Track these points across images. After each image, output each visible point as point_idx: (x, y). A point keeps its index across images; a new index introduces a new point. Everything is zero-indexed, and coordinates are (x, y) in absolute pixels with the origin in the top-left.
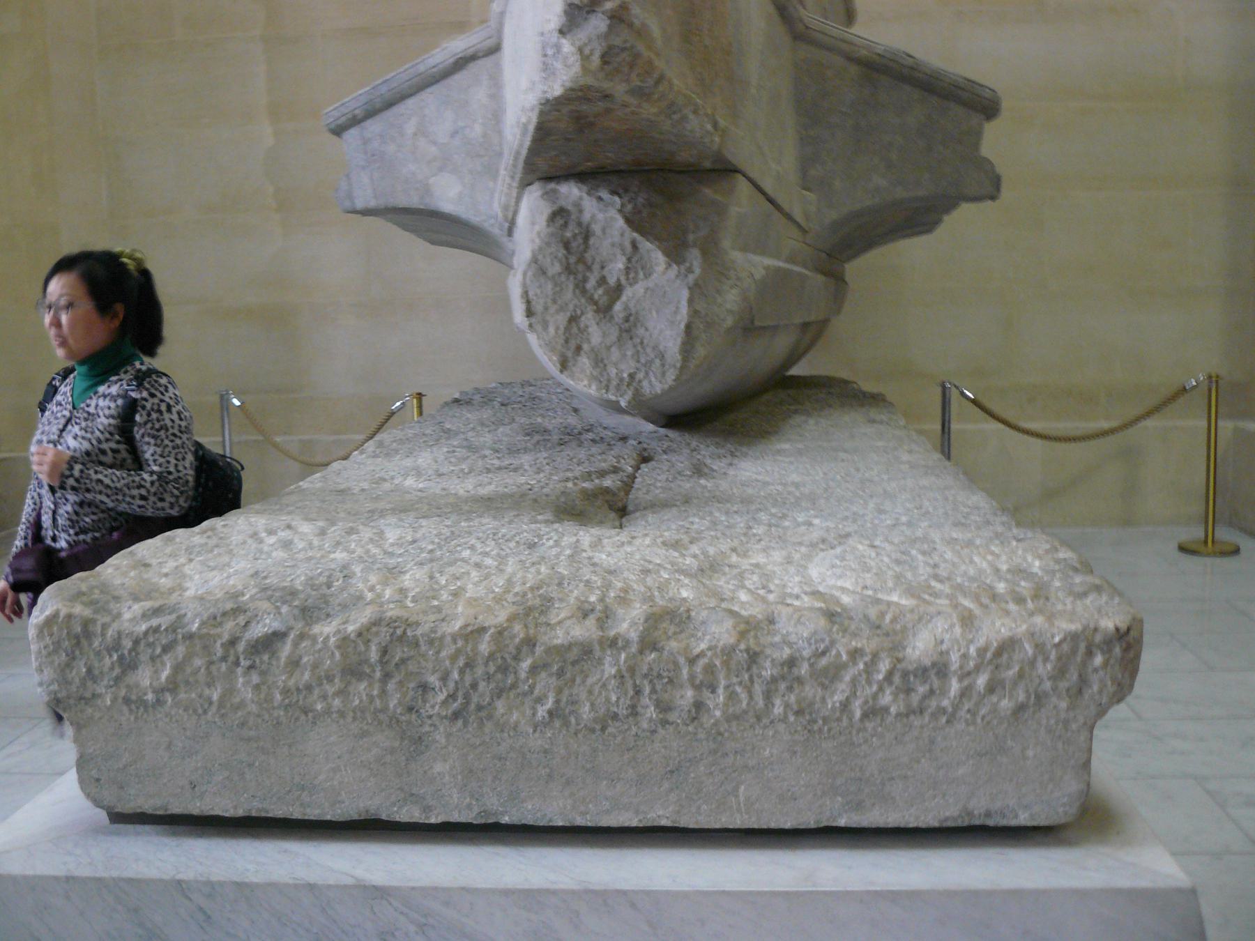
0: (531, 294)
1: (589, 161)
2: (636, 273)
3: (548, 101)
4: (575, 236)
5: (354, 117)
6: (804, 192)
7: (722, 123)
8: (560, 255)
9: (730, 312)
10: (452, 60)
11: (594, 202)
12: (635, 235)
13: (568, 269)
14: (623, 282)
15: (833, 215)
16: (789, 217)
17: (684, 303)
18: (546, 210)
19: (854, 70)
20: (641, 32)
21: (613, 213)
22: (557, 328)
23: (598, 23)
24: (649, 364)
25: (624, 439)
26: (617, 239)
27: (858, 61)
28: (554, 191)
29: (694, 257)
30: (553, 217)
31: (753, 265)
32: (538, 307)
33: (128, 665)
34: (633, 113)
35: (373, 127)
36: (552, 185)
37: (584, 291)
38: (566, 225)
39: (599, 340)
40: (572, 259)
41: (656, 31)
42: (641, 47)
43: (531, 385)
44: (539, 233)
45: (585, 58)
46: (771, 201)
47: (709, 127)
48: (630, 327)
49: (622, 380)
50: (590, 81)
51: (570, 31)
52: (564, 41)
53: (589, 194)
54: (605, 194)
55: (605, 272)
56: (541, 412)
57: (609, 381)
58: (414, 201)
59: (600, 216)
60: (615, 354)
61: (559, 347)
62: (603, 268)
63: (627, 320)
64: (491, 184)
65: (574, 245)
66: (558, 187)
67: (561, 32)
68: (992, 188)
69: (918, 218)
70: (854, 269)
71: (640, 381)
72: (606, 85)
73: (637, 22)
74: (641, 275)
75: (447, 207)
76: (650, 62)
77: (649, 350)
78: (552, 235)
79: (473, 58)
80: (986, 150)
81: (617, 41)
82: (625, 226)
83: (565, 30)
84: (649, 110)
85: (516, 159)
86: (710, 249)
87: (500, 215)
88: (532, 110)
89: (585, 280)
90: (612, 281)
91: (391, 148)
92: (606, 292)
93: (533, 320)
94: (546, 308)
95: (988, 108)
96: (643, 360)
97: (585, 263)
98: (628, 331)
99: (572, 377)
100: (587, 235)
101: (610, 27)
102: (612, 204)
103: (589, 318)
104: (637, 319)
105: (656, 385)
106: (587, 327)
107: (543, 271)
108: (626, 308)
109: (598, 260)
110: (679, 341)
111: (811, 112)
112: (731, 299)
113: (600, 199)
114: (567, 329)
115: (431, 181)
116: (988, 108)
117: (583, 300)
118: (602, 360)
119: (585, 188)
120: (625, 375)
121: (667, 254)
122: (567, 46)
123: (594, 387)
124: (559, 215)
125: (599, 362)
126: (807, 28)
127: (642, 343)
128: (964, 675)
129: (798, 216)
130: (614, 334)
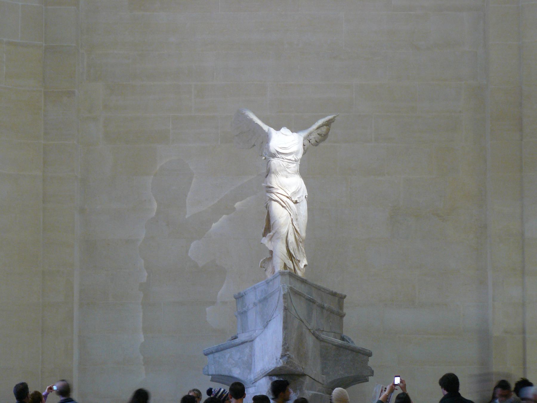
15: (330, 380)
19: (334, 347)
23: (286, 358)
27: (335, 345)
29: (298, 391)
35: (217, 355)
41: (293, 356)
58: (226, 373)
64: (248, 371)
79: (246, 342)
84: (292, 368)
87: (253, 379)
95: (370, 355)
111: (324, 357)
116: (370, 355)
129: (321, 381)
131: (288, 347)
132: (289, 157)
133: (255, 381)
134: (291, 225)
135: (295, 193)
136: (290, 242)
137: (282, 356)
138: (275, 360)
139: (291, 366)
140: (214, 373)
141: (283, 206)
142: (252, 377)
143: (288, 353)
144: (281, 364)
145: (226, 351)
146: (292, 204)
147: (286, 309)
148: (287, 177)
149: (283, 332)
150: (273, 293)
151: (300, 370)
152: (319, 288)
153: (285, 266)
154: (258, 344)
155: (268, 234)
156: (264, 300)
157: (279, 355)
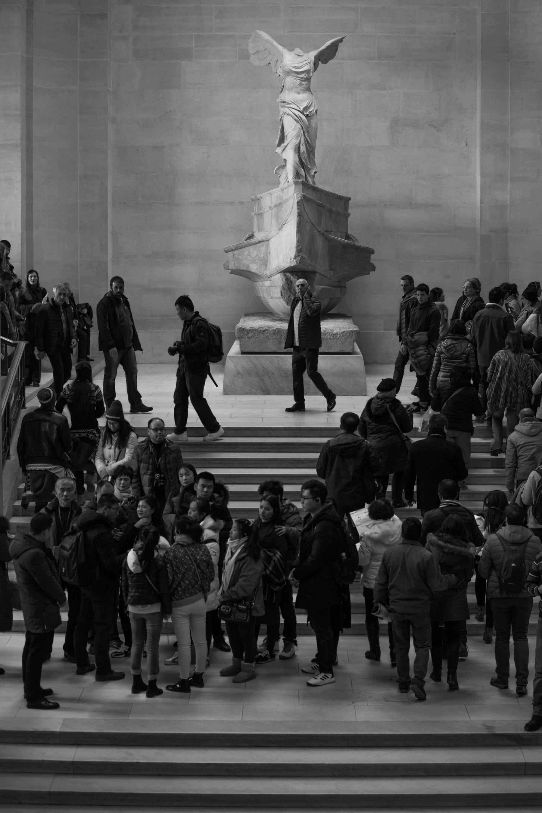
13: (288, 288)
30: (286, 280)
33: (248, 333)
35: (236, 252)
58: (245, 269)
68: (374, 269)
70: (349, 284)
75: (253, 271)
84: (304, 267)
87: (268, 274)
91: (240, 257)
95: (372, 252)
100: (292, 282)
116: (372, 252)
124: (287, 279)
128: (340, 335)
129: (328, 276)
131: (301, 249)
132: (302, 76)
133: (271, 276)
134: (303, 137)
135: (306, 108)
136: (301, 151)
137: (295, 257)
139: (303, 265)
140: (234, 268)
141: (295, 120)
142: (268, 273)
144: (294, 263)
145: (244, 249)
146: (304, 117)
147: (300, 215)
148: (299, 94)
150: (287, 200)
151: (310, 268)
152: (327, 194)
153: (297, 175)
154: (273, 244)
155: (283, 145)
156: (279, 205)
157: (293, 257)
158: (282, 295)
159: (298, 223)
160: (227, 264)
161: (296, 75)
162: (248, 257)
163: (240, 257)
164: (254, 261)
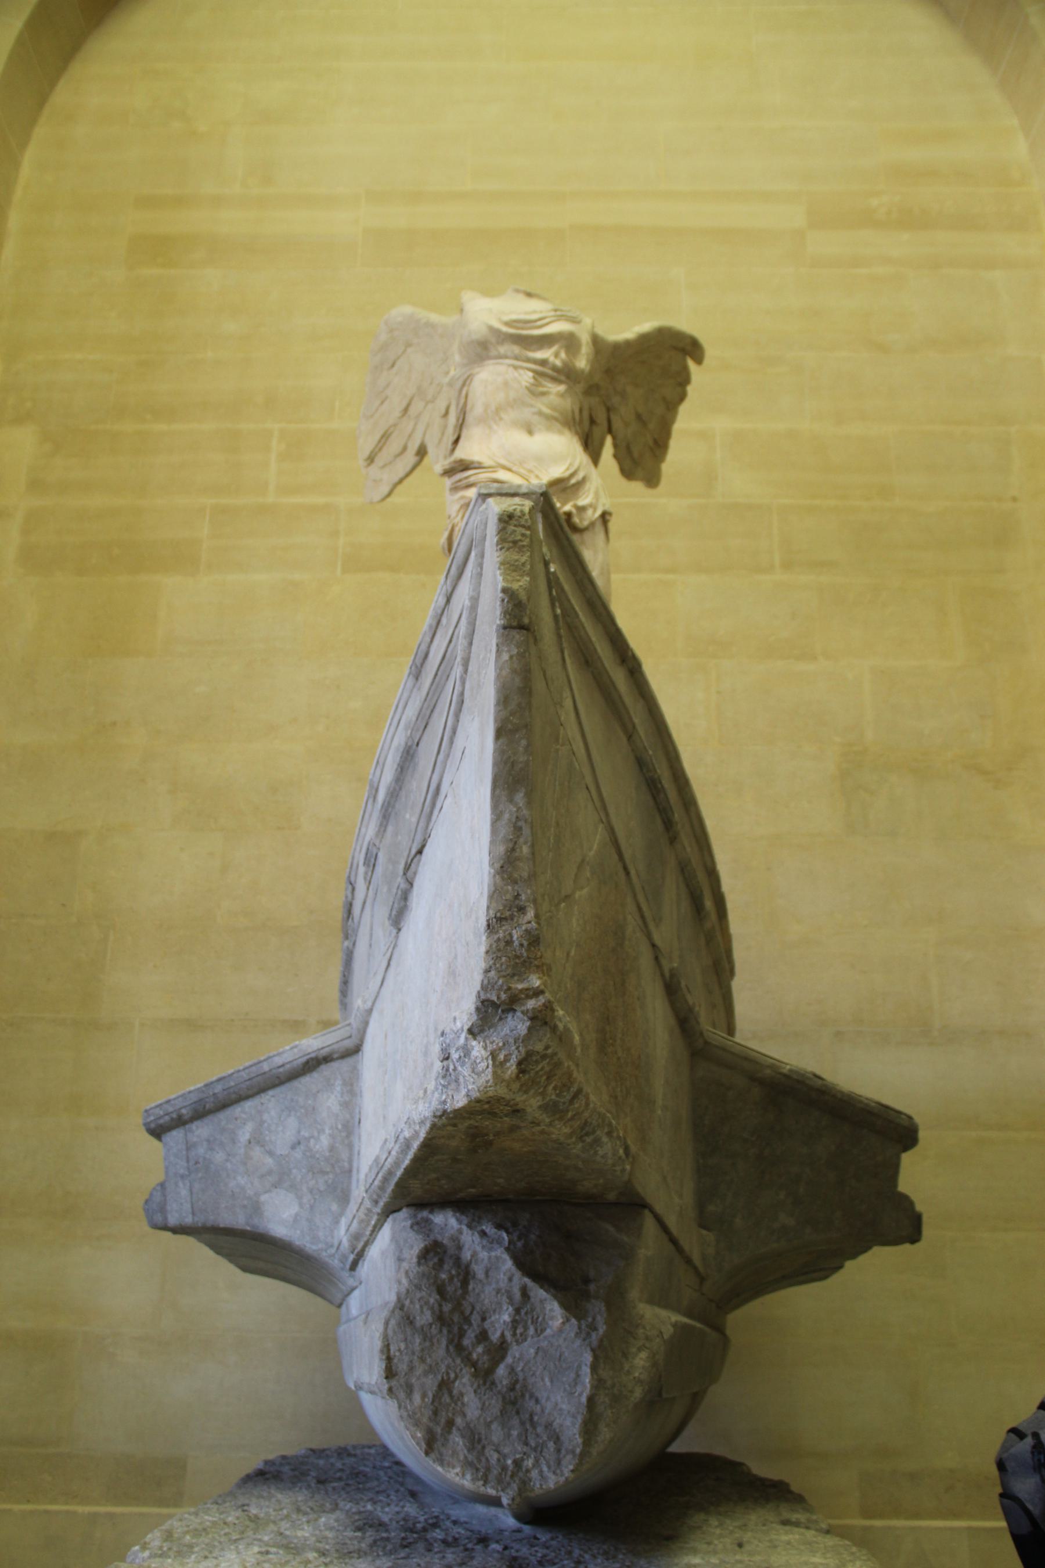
0: (392, 1348)
1: (473, 1187)
2: (526, 1328)
3: (445, 1112)
4: (451, 1278)
5: (180, 1117)
6: (704, 1232)
7: (633, 1149)
8: (432, 1300)
9: (640, 1381)
10: (304, 1059)
11: (477, 1237)
12: (526, 1280)
13: (441, 1319)
14: (508, 1335)
16: (689, 1261)
17: (586, 1370)
18: (416, 1244)
20: (563, 1038)
21: (500, 1252)
22: (424, 1396)
23: (517, 1025)
24: (539, 1449)
25: (484, 1540)
26: (503, 1284)
28: (427, 1221)
30: (424, 1256)
31: (659, 1320)
32: (402, 1367)
34: (542, 1132)
35: (201, 1130)
36: (425, 1214)
37: (460, 1348)
38: (441, 1262)
39: (477, 1413)
40: (447, 1307)
42: (562, 1055)
43: (349, 1455)
44: (407, 1273)
45: (499, 1066)
46: (673, 1241)
47: (621, 1151)
48: (515, 1400)
49: (504, 1468)
50: (502, 1091)
51: (482, 1031)
52: (474, 1043)
53: (469, 1227)
54: (489, 1228)
55: (487, 1325)
56: (370, 1495)
57: (488, 1469)
58: (239, 1220)
59: (483, 1255)
60: (497, 1434)
61: (425, 1420)
62: (484, 1319)
63: (512, 1388)
64: (335, 1207)
65: (450, 1289)
66: (431, 1216)
67: (470, 1031)
69: (818, 1264)
70: (737, 1320)
71: (528, 1471)
72: (520, 1098)
73: (561, 1026)
74: (531, 1331)
75: (279, 1230)
76: (569, 1074)
77: (539, 1430)
78: (424, 1275)
79: (327, 1059)
80: (904, 1185)
81: (539, 1047)
82: (514, 1268)
83: (476, 1030)
84: (561, 1131)
85: (385, 1180)
86: (616, 1299)
87: (345, 1243)
88: (422, 1123)
89: (462, 1334)
90: (495, 1337)
91: (219, 1157)
92: (487, 1351)
93: (394, 1383)
94: (411, 1368)
96: (533, 1444)
97: (462, 1313)
98: (514, 1403)
99: (441, 1461)
100: (466, 1275)
101: (530, 1029)
102: (499, 1242)
103: (465, 1384)
104: (525, 1386)
105: (550, 1479)
106: (462, 1395)
107: (408, 1320)
108: (512, 1370)
109: (478, 1308)
110: (580, 1419)
112: (640, 1361)
113: (483, 1234)
114: (436, 1397)
115: (263, 1198)
117: (458, 1361)
118: (480, 1440)
119: (465, 1220)
120: (509, 1462)
121: (564, 1305)
122: (478, 1050)
123: (468, 1477)
124: (435, 1252)
125: (475, 1441)
126: (706, 1043)
127: (531, 1419)
129: (696, 1259)
130: (495, 1405)
131: (534, 940)
132: (540, 355)
137: (490, 1012)
138: (438, 1065)
143: (535, 981)
144: (473, 1082)
145: (237, 1110)
148: (530, 432)
149: (497, 815)
158: (390, 1373)
159: (504, 700)
160: (158, 1197)
161: (516, 349)
162: (257, 1152)
163: (219, 1157)
164: (281, 1179)
